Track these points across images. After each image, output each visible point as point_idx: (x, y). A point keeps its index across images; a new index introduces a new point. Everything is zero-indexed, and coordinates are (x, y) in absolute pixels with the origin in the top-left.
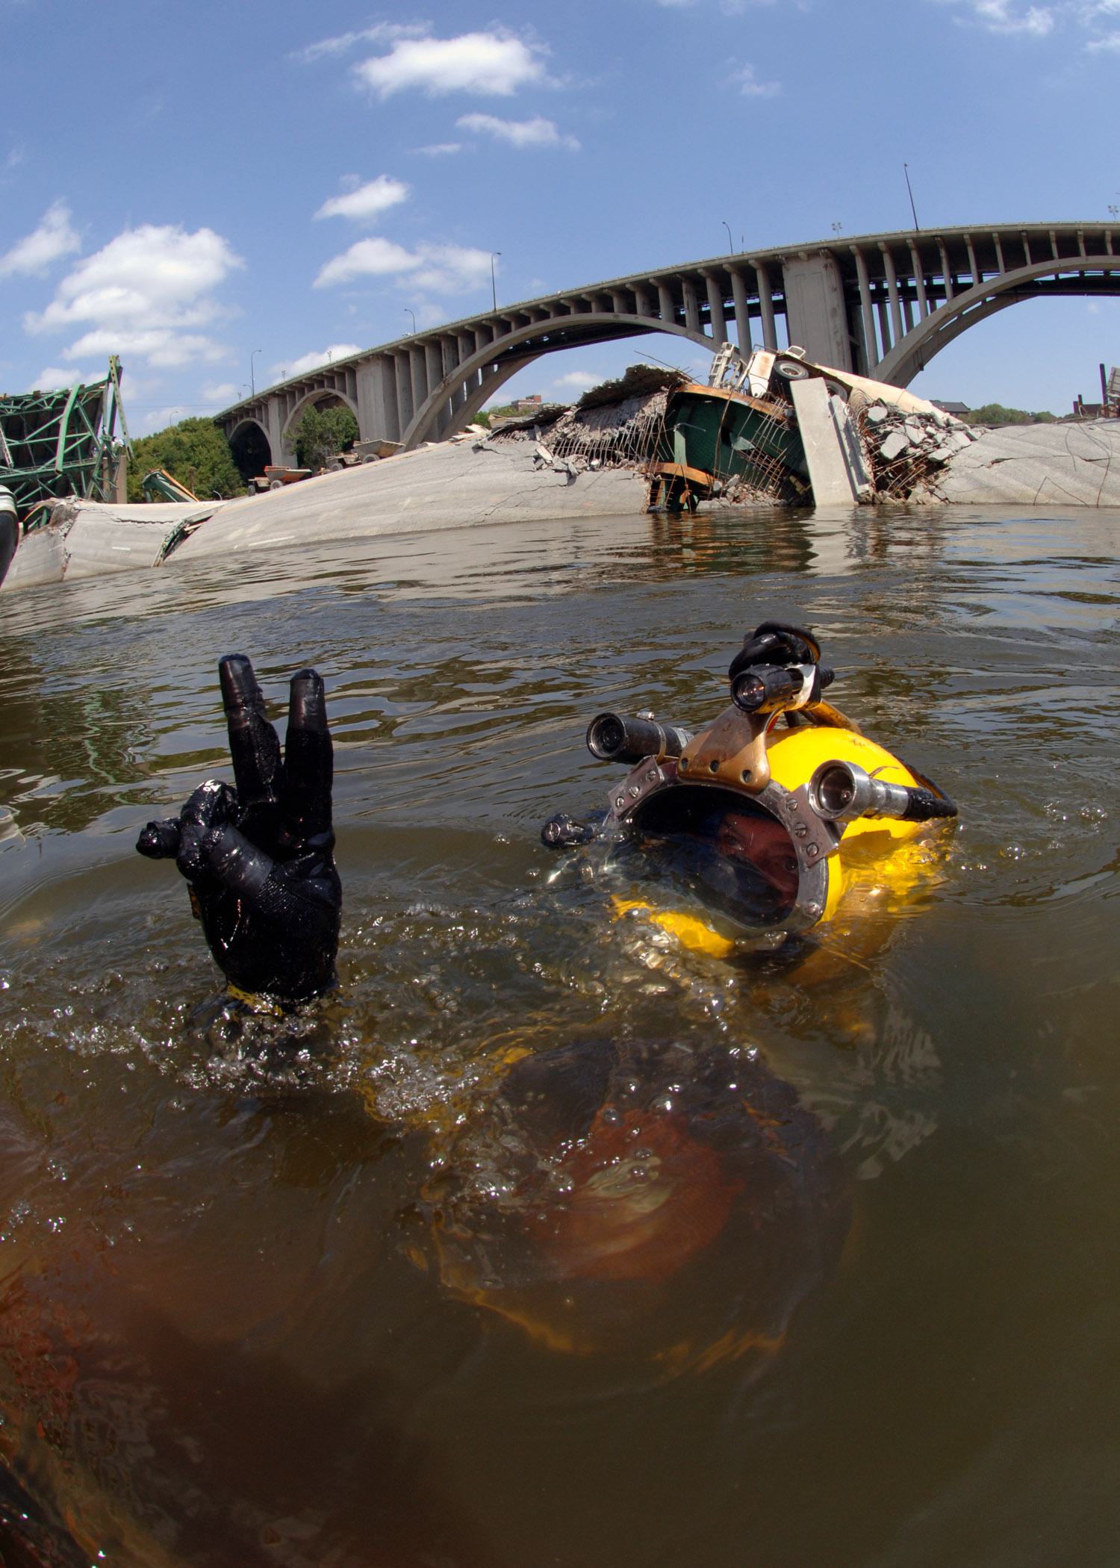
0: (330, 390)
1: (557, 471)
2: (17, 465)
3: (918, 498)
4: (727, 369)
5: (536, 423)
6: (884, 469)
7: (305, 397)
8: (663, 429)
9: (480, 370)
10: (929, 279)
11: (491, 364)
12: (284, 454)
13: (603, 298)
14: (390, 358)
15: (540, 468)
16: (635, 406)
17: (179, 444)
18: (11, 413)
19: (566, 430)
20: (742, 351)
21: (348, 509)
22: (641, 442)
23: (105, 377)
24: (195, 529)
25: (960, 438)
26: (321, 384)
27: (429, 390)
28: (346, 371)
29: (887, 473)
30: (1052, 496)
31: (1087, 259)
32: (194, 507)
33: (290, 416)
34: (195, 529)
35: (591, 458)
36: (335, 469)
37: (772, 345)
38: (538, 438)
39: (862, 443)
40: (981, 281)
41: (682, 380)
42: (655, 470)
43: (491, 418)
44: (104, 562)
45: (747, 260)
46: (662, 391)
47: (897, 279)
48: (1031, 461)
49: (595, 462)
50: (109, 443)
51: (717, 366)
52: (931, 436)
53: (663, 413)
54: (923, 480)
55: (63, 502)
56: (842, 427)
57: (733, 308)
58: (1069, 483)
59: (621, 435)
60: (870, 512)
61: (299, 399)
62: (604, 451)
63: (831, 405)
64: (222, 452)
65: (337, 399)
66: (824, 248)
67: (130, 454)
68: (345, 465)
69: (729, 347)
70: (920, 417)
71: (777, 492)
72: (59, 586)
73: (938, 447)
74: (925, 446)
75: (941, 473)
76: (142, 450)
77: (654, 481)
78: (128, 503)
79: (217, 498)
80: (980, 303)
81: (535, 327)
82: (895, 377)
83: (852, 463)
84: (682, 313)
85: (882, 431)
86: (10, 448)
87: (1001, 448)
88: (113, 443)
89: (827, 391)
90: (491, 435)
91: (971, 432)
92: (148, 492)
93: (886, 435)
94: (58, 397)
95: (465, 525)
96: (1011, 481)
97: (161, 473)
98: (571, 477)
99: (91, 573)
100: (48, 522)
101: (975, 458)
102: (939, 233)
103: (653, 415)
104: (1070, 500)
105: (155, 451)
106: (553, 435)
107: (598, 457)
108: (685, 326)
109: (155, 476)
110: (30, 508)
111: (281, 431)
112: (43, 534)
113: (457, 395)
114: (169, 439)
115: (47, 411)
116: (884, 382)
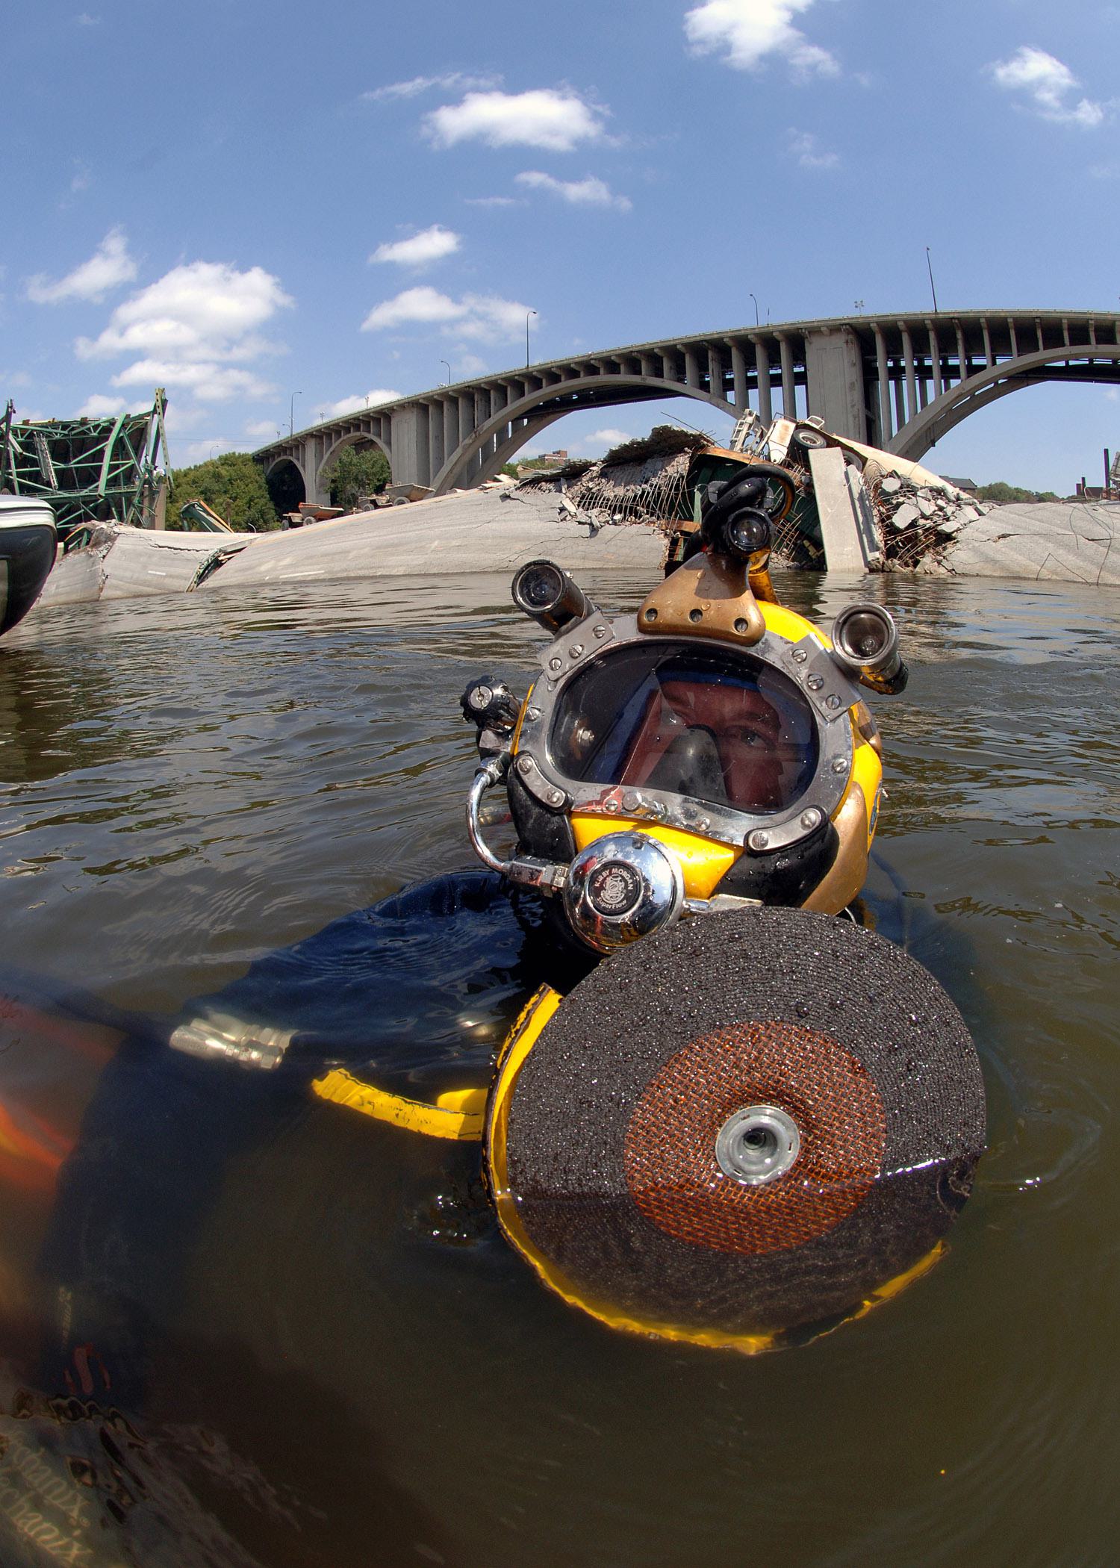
0: (366, 435)
1: (580, 523)
2: (61, 487)
3: (926, 567)
4: (748, 434)
5: (563, 476)
6: (895, 538)
8: (684, 489)
9: (510, 423)
10: (945, 360)
11: (521, 418)
12: (319, 493)
13: (632, 360)
14: (424, 407)
15: (564, 519)
16: (659, 464)
17: (217, 477)
18: (58, 436)
19: (591, 485)
20: (762, 419)
21: (378, 548)
22: (663, 500)
23: (152, 409)
24: (229, 559)
25: (969, 512)
26: (358, 428)
27: (461, 440)
28: (382, 417)
29: (897, 542)
30: (1054, 572)
31: (1097, 348)
32: (229, 538)
33: (326, 457)
34: (229, 559)
35: (614, 513)
36: (367, 509)
37: (791, 414)
38: (564, 491)
39: (875, 512)
40: (994, 363)
41: (705, 443)
42: (675, 527)
43: (519, 469)
44: (140, 585)
45: (772, 333)
46: (685, 452)
47: (914, 357)
48: (1036, 538)
49: (618, 517)
50: (150, 472)
51: (739, 431)
52: (941, 509)
53: (685, 474)
54: (932, 551)
55: (103, 525)
56: (856, 495)
57: (756, 377)
58: (1071, 560)
59: (643, 492)
60: (878, 579)
62: (626, 507)
63: (846, 474)
64: (260, 487)
65: (372, 442)
66: (846, 324)
67: (170, 483)
68: (377, 507)
69: (750, 414)
70: (932, 490)
71: (790, 554)
72: (91, 605)
73: (948, 520)
74: (935, 518)
75: (949, 545)
76: (182, 480)
77: (673, 538)
78: (166, 530)
79: (251, 530)
80: (992, 385)
81: (565, 385)
82: (907, 452)
83: (864, 530)
84: (707, 379)
85: (894, 502)
86: (55, 470)
87: (1007, 523)
88: (155, 472)
89: (843, 461)
90: (519, 485)
91: (979, 507)
92: (187, 520)
93: (898, 505)
94: (104, 424)
95: (489, 570)
96: (1015, 556)
97: (199, 503)
98: (594, 530)
99: (125, 595)
100: (88, 543)
101: (982, 532)
102: (956, 315)
103: (675, 475)
104: (1071, 577)
105: (194, 482)
106: (578, 488)
107: (620, 512)
108: (709, 392)
109: (193, 505)
110: (71, 529)
111: (316, 470)
112: (83, 554)
113: (486, 447)
114: (209, 472)
115: (93, 437)
116: (897, 455)
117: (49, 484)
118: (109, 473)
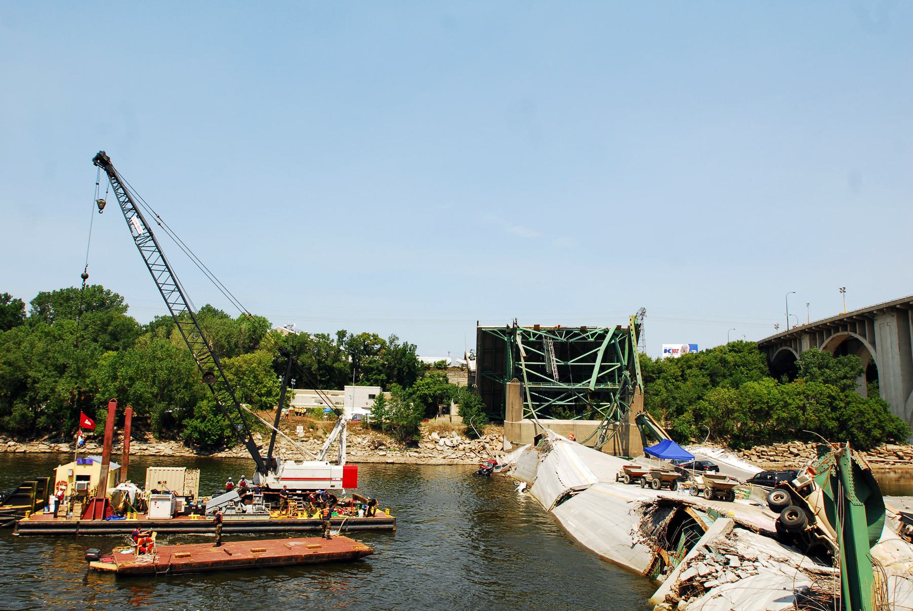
0: (853, 334)
7: (831, 337)
61: (827, 338)
94: (600, 332)
115: (591, 342)
117: (551, 376)
118: (599, 373)
